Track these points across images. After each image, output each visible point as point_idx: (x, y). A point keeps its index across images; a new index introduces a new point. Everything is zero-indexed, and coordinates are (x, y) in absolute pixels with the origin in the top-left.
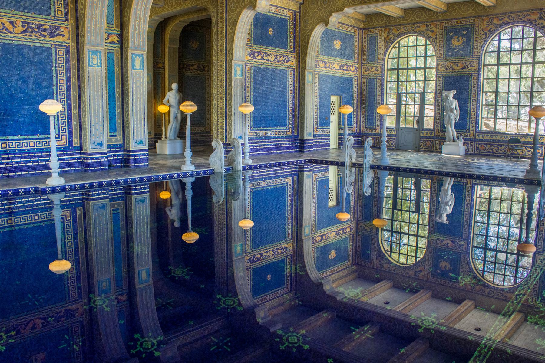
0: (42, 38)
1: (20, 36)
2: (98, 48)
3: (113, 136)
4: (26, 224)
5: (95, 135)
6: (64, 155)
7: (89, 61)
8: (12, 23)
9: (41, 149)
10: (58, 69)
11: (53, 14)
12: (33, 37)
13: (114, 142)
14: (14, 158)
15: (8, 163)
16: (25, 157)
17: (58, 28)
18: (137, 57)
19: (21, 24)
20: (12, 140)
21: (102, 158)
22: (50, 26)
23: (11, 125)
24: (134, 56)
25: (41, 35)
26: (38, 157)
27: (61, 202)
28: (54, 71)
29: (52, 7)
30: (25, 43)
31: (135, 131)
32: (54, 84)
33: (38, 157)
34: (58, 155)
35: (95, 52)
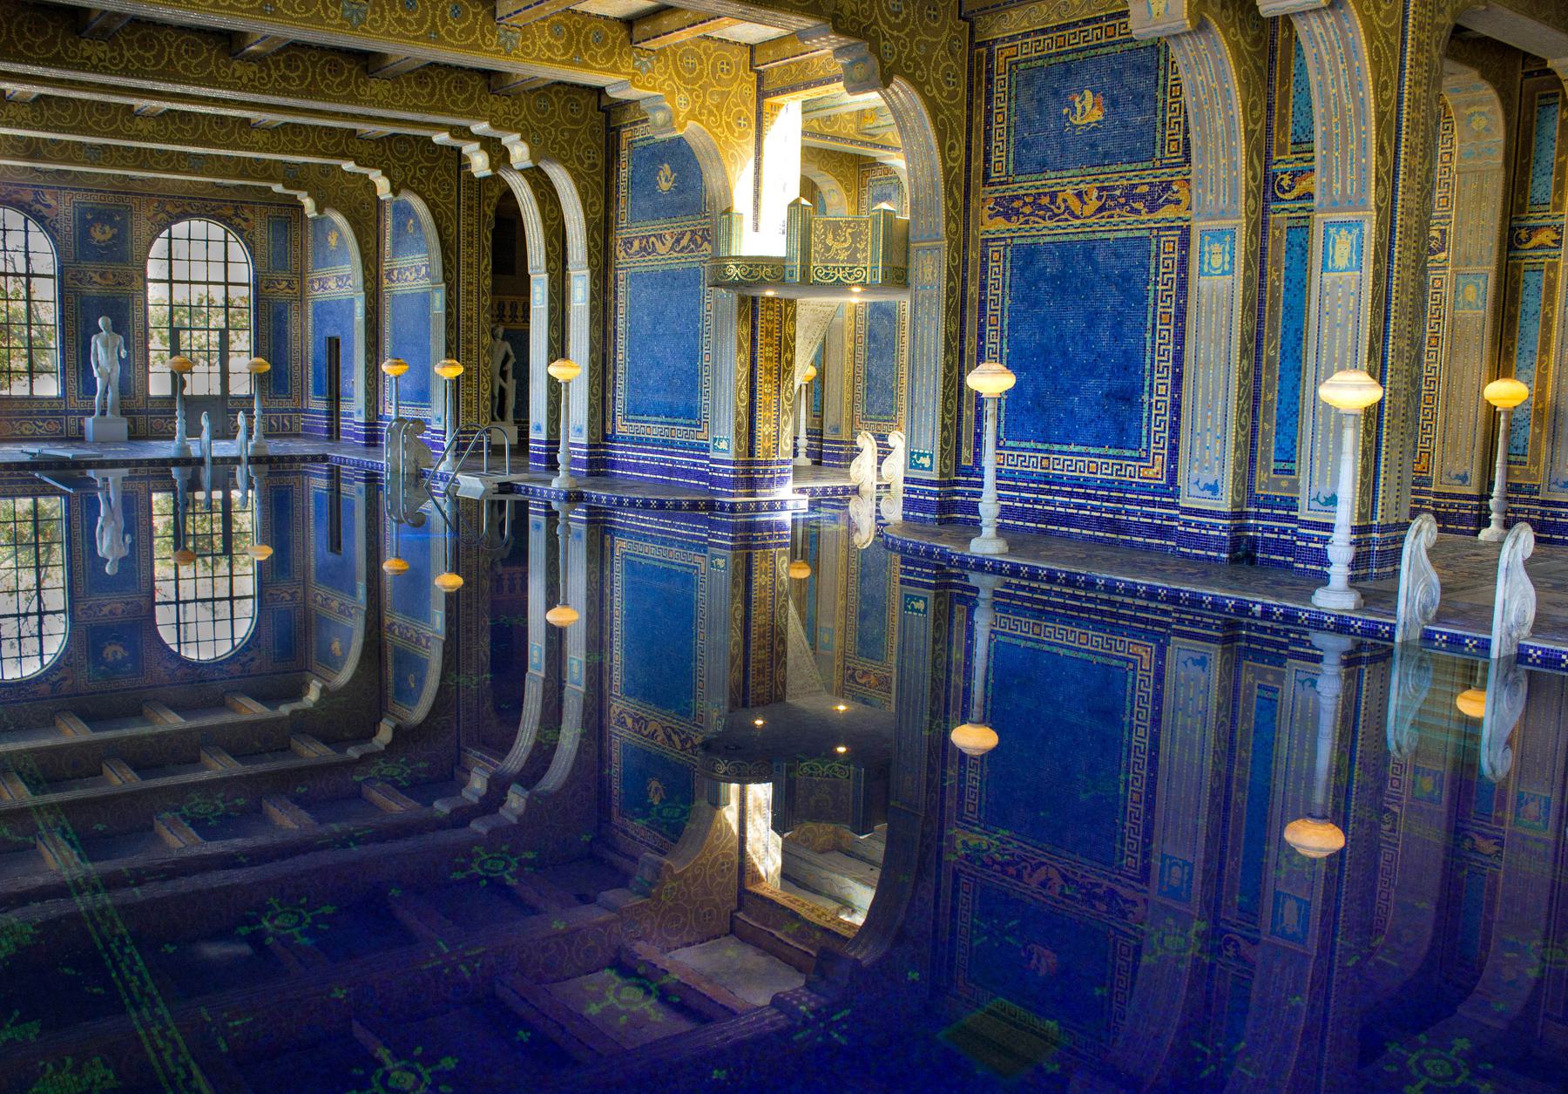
0: (1133, 217)
1: (1093, 220)
2: (1226, 224)
3: (1283, 471)
4: (1062, 646)
5: (1202, 460)
6: (1153, 504)
7: (1202, 262)
8: (1079, 195)
9: (1108, 481)
10: (1160, 287)
11: (1158, 155)
12: (1116, 219)
13: (1286, 490)
14: (1058, 493)
15: (1048, 503)
16: (1078, 495)
17: (1167, 186)
18: (1343, 232)
19: (1095, 194)
20: (1060, 452)
21: (1214, 527)
22: (1151, 184)
23: (1061, 420)
24: (1332, 231)
25: (1134, 211)
26: (1102, 498)
27: (996, 594)
28: (1151, 294)
29: (1158, 136)
30: (1099, 235)
31: (1317, 464)
32: (1149, 325)
33: (1102, 498)
34: (999, 487)
35: (1218, 235)
